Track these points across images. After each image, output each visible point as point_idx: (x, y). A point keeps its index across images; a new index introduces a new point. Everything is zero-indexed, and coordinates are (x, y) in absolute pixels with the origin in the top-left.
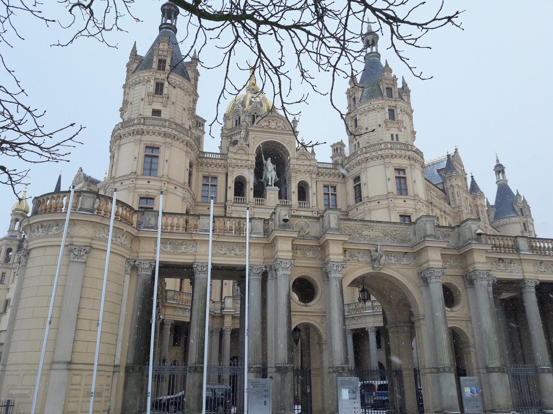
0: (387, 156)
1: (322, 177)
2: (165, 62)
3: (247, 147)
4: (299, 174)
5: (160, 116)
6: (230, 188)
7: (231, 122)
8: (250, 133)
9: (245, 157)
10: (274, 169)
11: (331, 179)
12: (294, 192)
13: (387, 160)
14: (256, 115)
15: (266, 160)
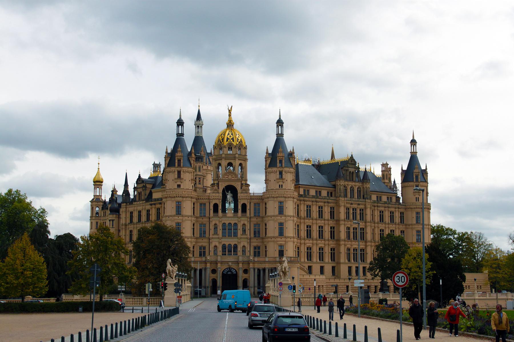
0: (275, 197)
1: (253, 201)
2: (180, 160)
3: (218, 189)
4: (242, 200)
5: (180, 187)
6: (211, 209)
7: (217, 150)
8: (219, 182)
9: (217, 195)
10: (232, 196)
11: (257, 201)
12: (239, 209)
13: (275, 199)
14: (230, 147)
15: (228, 192)
